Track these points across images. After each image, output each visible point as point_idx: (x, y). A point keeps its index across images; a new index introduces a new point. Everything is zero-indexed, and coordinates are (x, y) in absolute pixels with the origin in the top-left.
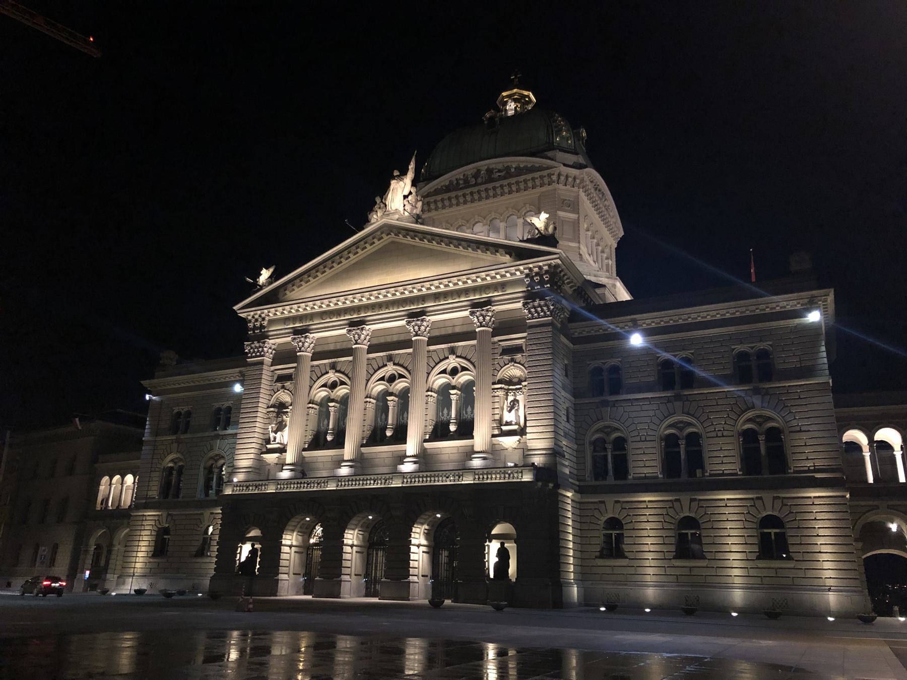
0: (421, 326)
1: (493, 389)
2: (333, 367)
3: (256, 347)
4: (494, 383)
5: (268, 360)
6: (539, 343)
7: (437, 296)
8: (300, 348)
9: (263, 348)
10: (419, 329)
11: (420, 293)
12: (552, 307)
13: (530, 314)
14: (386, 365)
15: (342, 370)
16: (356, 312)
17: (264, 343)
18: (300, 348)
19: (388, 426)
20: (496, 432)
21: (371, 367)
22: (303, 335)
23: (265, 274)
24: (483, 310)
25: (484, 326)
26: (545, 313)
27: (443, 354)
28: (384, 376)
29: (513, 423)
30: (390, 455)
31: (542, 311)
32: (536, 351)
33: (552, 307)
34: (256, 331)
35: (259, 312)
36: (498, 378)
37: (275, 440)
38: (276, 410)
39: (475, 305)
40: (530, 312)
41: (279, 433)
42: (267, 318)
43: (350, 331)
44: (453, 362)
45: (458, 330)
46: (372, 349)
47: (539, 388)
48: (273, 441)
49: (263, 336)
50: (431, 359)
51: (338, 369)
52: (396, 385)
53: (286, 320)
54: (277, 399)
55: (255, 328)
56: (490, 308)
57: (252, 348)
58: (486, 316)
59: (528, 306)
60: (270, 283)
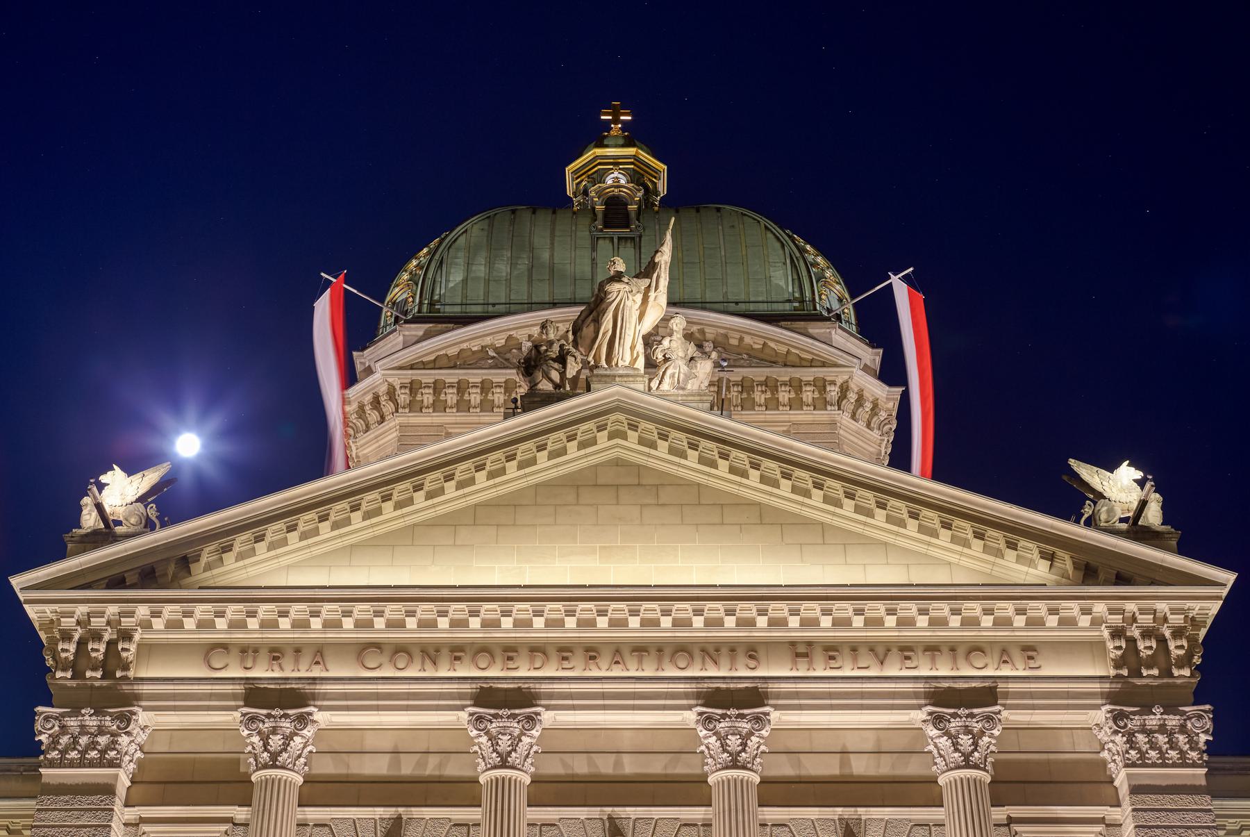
0: (751, 734)
3: (83, 730)
5: (124, 781)
7: (800, 651)
8: (274, 756)
10: (744, 745)
12: (1203, 738)
13: (1131, 748)
16: (499, 661)
17: (126, 719)
18: (274, 756)
22: (290, 712)
24: (972, 716)
25: (976, 767)
26: (1182, 753)
31: (1173, 745)
34: (89, 674)
35: (112, 609)
40: (1131, 743)
43: (480, 719)
45: (861, 767)
57: (63, 727)
58: (982, 733)
59: (1126, 725)
60: (149, 526)
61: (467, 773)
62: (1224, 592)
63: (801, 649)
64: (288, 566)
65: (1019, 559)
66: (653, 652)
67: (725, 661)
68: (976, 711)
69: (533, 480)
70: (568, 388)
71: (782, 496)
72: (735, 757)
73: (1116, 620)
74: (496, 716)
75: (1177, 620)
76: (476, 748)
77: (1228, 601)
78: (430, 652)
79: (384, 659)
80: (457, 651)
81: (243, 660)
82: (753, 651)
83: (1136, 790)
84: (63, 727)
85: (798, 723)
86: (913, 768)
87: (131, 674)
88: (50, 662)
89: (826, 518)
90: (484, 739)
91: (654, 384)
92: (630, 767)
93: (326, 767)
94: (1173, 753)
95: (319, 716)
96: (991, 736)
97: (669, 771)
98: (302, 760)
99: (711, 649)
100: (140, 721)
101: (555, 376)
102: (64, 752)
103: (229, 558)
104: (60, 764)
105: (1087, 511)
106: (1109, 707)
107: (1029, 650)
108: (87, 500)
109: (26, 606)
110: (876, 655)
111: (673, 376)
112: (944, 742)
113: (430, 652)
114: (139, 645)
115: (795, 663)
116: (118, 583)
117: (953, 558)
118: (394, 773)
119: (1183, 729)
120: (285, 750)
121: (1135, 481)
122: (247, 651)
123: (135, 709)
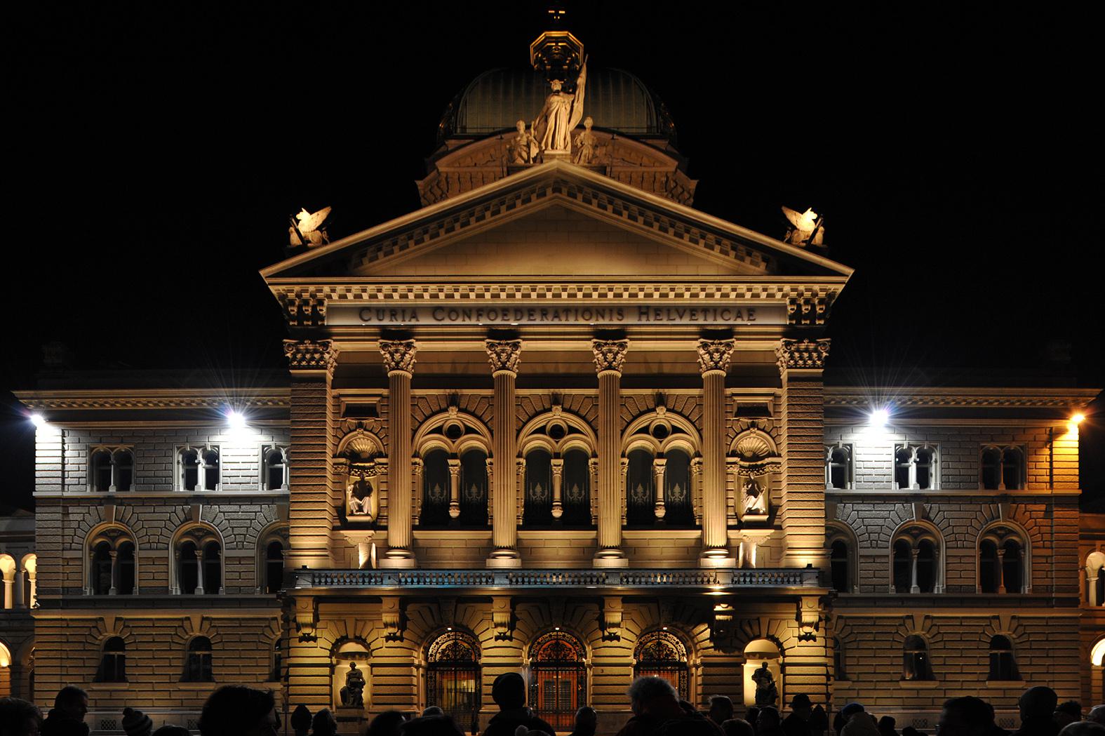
0: (618, 353)
2: (453, 401)
3: (307, 351)
4: (728, 455)
5: (330, 377)
6: (805, 405)
7: (643, 311)
8: (397, 363)
9: (322, 353)
10: (615, 358)
11: (617, 301)
12: (825, 354)
13: (792, 359)
14: (550, 410)
17: (326, 345)
18: (397, 363)
19: (554, 504)
20: (732, 522)
21: (521, 410)
23: (308, 222)
24: (721, 344)
25: (720, 369)
26: (814, 362)
27: (644, 403)
28: (544, 427)
29: (761, 512)
30: (566, 544)
31: (810, 358)
32: (801, 415)
33: (825, 354)
34: (305, 323)
37: (360, 508)
38: (348, 462)
39: (707, 334)
40: (792, 357)
41: (367, 499)
42: (326, 303)
47: (805, 468)
48: (357, 511)
49: (322, 335)
50: (625, 409)
51: (463, 406)
52: (566, 442)
53: (362, 311)
54: (349, 444)
55: (301, 316)
56: (733, 342)
57: (298, 351)
58: (724, 352)
60: (324, 243)
62: (846, 280)
63: (644, 310)
64: (396, 265)
65: (752, 263)
66: (573, 311)
67: (607, 316)
68: (723, 341)
69: (514, 217)
70: (532, 162)
72: (610, 363)
73: (794, 294)
74: (499, 344)
75: (822, 295)
76: (491, 360)
77: (848, 285)
78: (467, 312)
80: (480, 311)
82: (620, 311)
83: (791, 379)
85: (640, 348)
86: (691, 370)
88: (287, 317)
89: (659, 240)
90: (494, 356)
91: (577, 158)
92: (562, 369)
94: (810, 362)
95: (416, 344)
96: (729, 354)
98: (411, 366)
100: (333, 347)
101: (525, 155)
102: (300, 362)
103: (366, 260)
104: (300, 367)
105: (788, 236)
106: (784, 339)
107: (751, 311)
108: (292, 229)
109: (269, 287)
110: (678, 313)
111: (585, 156)
112: (707, 357)
113: (467, 312)
114: (328, 308)
117: (720, 262)
119: (816, 350)
120: (402, 361)
121: (813, 220)
123: (329, 340)
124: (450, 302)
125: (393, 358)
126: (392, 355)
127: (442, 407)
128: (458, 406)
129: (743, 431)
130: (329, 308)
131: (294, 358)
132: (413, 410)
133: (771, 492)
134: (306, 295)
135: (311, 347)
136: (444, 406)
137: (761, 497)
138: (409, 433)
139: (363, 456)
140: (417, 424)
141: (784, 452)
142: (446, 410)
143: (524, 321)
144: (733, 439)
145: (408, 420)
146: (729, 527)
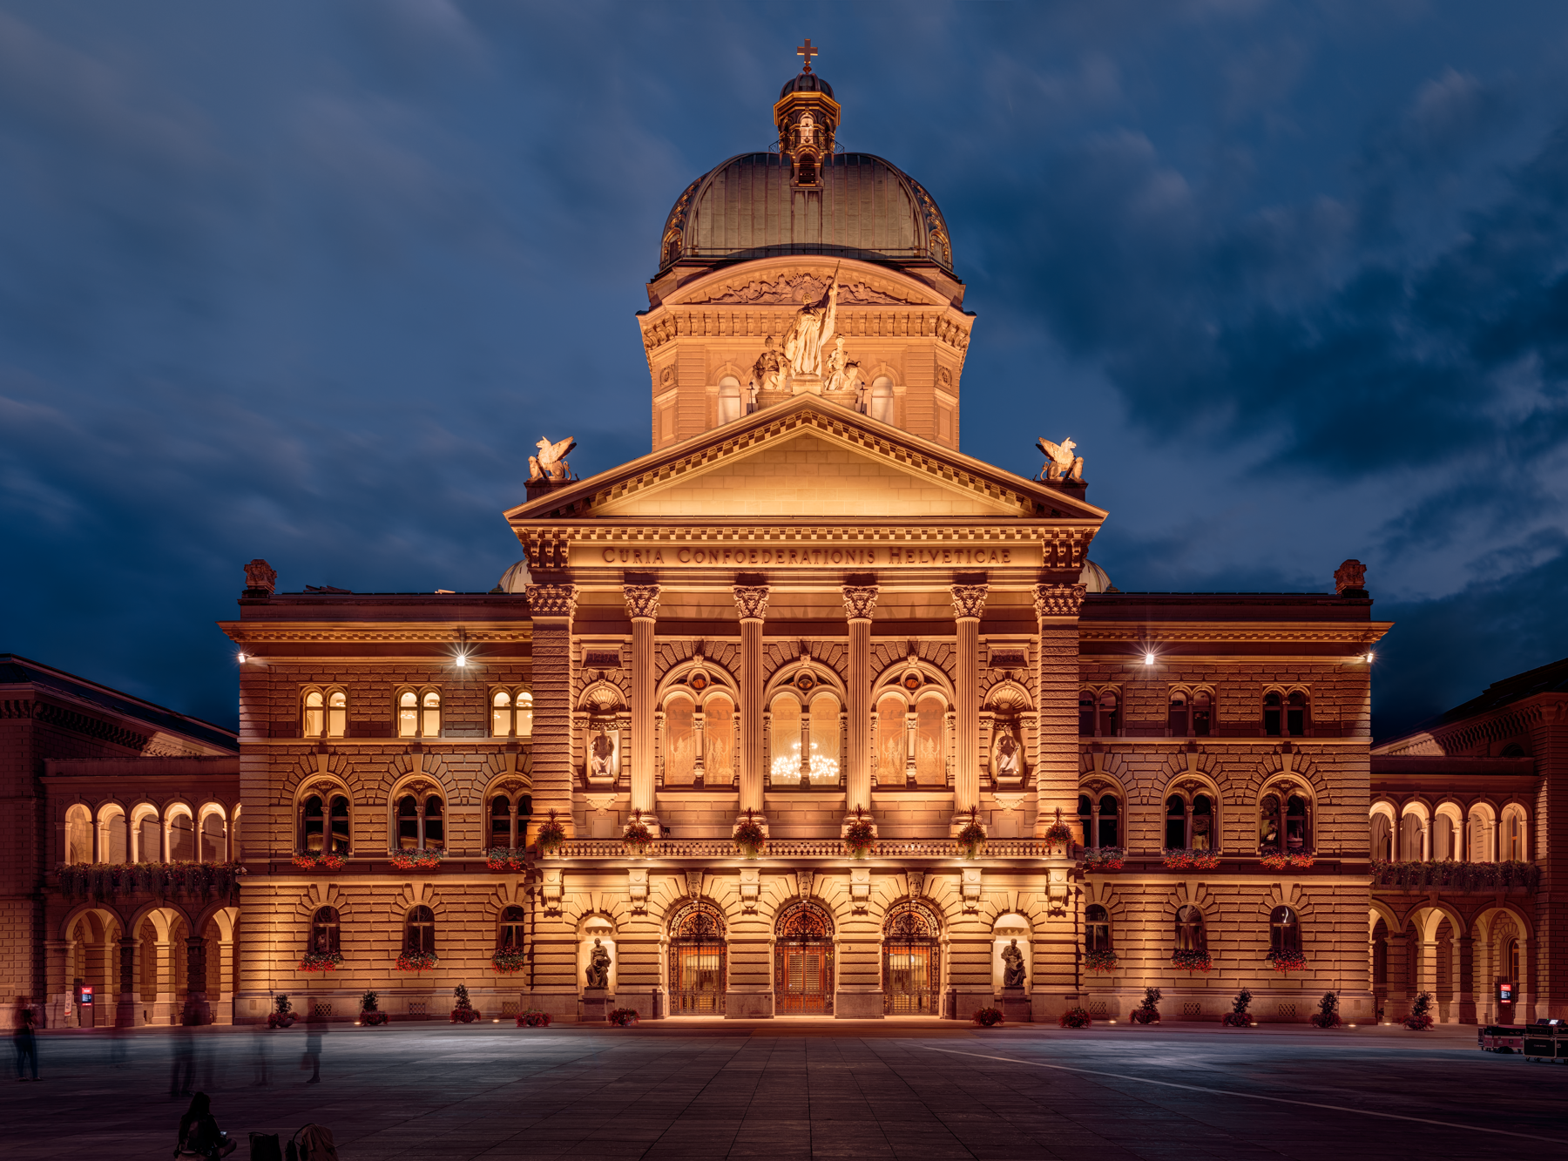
1: (981, 718)
2: (700, 649)
3: (549, 597)
4: (981, 709)
5: (571, 621)
8: (642, 610)
9: (564, 598)
10: (865, 605)
14: (798, 659)
15: (716, 657)
17: (569, 590)
34: (548, 565)
36: (986, 701)
42: (568, 544)
43: (740, 591)
44: (913, 666)
45: (921, 613)
46: (773, 627)
51: (708, 654)
53: (606, 551)
55: (542, 559)
57: (539, 594)
61: (733, 617)
66: (823, 552)
71: (890, 460)
72: (860, 611)
74: (747, 590)
79: (691, 557)
81: (621, 557)
84: (539, 594)
87: (568, 565)
90: (742, 602)
92: (811, 614)
93: (666, 613)
97: (830, 616)
99: (851, 552)
103: (609, 498)
115: (892, 559)
116: (555, 514)
118: (698, 617)
122: (623, 552)
124: (697, 543)
125: (637, 604)
126: (636, 600)
127: (687, 655)
128: (703, 654)
129: (998, 682)
130: (571, 548)
131: (536, 600)
132: (657, 658)
133: (1027, 750)
134: (549, 536)
135: (553, 592)
136: (688, 654)
137: (1014, 756)
138: (654, 684)
139: (603, 707)
140: (661, 674)
141: (1039, 707)
142: (691, 659)
143: (772, 565)
144: (987, 691)
145: (652, 668)
146: (982, 789)
